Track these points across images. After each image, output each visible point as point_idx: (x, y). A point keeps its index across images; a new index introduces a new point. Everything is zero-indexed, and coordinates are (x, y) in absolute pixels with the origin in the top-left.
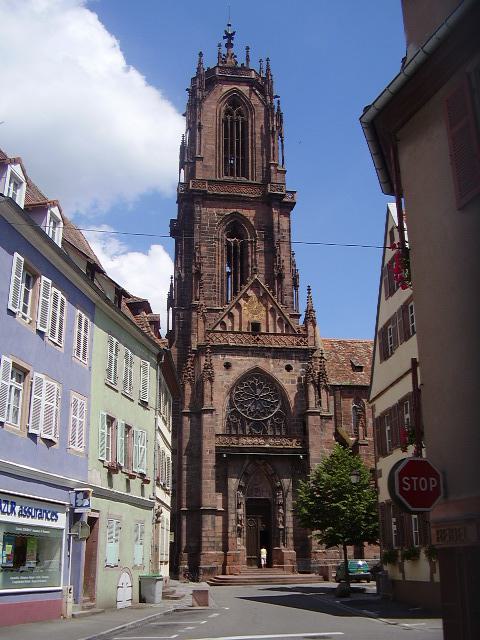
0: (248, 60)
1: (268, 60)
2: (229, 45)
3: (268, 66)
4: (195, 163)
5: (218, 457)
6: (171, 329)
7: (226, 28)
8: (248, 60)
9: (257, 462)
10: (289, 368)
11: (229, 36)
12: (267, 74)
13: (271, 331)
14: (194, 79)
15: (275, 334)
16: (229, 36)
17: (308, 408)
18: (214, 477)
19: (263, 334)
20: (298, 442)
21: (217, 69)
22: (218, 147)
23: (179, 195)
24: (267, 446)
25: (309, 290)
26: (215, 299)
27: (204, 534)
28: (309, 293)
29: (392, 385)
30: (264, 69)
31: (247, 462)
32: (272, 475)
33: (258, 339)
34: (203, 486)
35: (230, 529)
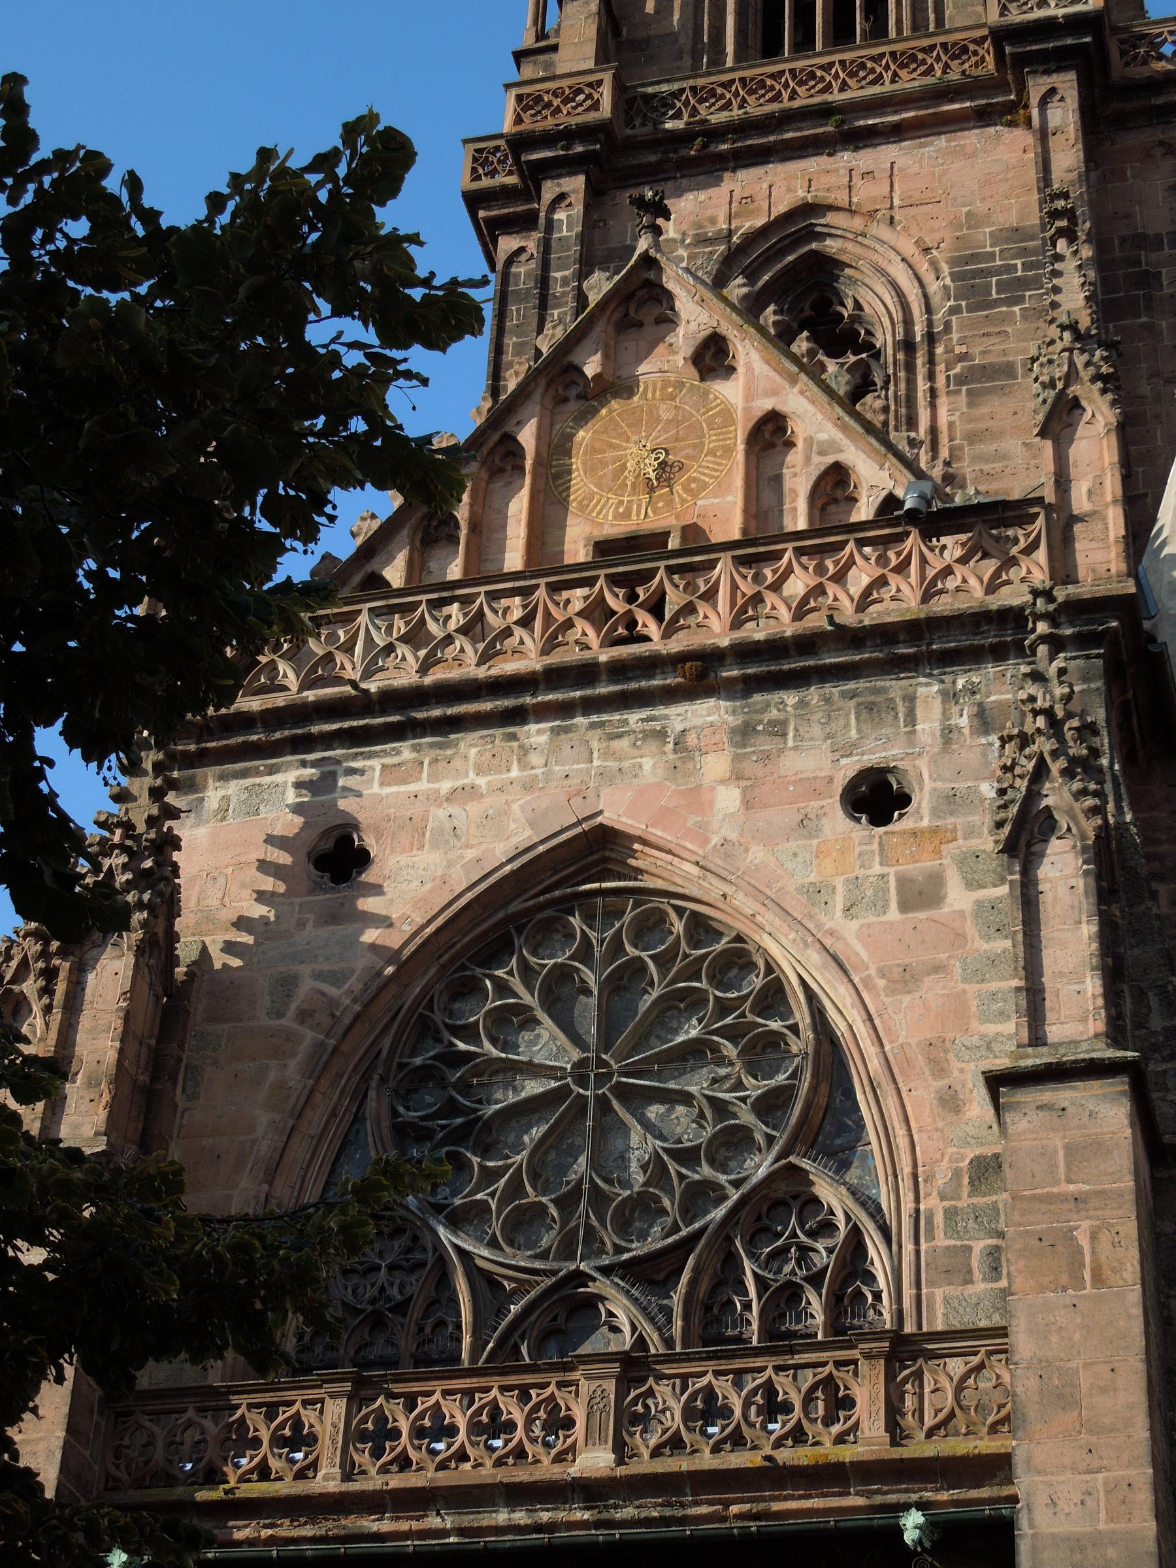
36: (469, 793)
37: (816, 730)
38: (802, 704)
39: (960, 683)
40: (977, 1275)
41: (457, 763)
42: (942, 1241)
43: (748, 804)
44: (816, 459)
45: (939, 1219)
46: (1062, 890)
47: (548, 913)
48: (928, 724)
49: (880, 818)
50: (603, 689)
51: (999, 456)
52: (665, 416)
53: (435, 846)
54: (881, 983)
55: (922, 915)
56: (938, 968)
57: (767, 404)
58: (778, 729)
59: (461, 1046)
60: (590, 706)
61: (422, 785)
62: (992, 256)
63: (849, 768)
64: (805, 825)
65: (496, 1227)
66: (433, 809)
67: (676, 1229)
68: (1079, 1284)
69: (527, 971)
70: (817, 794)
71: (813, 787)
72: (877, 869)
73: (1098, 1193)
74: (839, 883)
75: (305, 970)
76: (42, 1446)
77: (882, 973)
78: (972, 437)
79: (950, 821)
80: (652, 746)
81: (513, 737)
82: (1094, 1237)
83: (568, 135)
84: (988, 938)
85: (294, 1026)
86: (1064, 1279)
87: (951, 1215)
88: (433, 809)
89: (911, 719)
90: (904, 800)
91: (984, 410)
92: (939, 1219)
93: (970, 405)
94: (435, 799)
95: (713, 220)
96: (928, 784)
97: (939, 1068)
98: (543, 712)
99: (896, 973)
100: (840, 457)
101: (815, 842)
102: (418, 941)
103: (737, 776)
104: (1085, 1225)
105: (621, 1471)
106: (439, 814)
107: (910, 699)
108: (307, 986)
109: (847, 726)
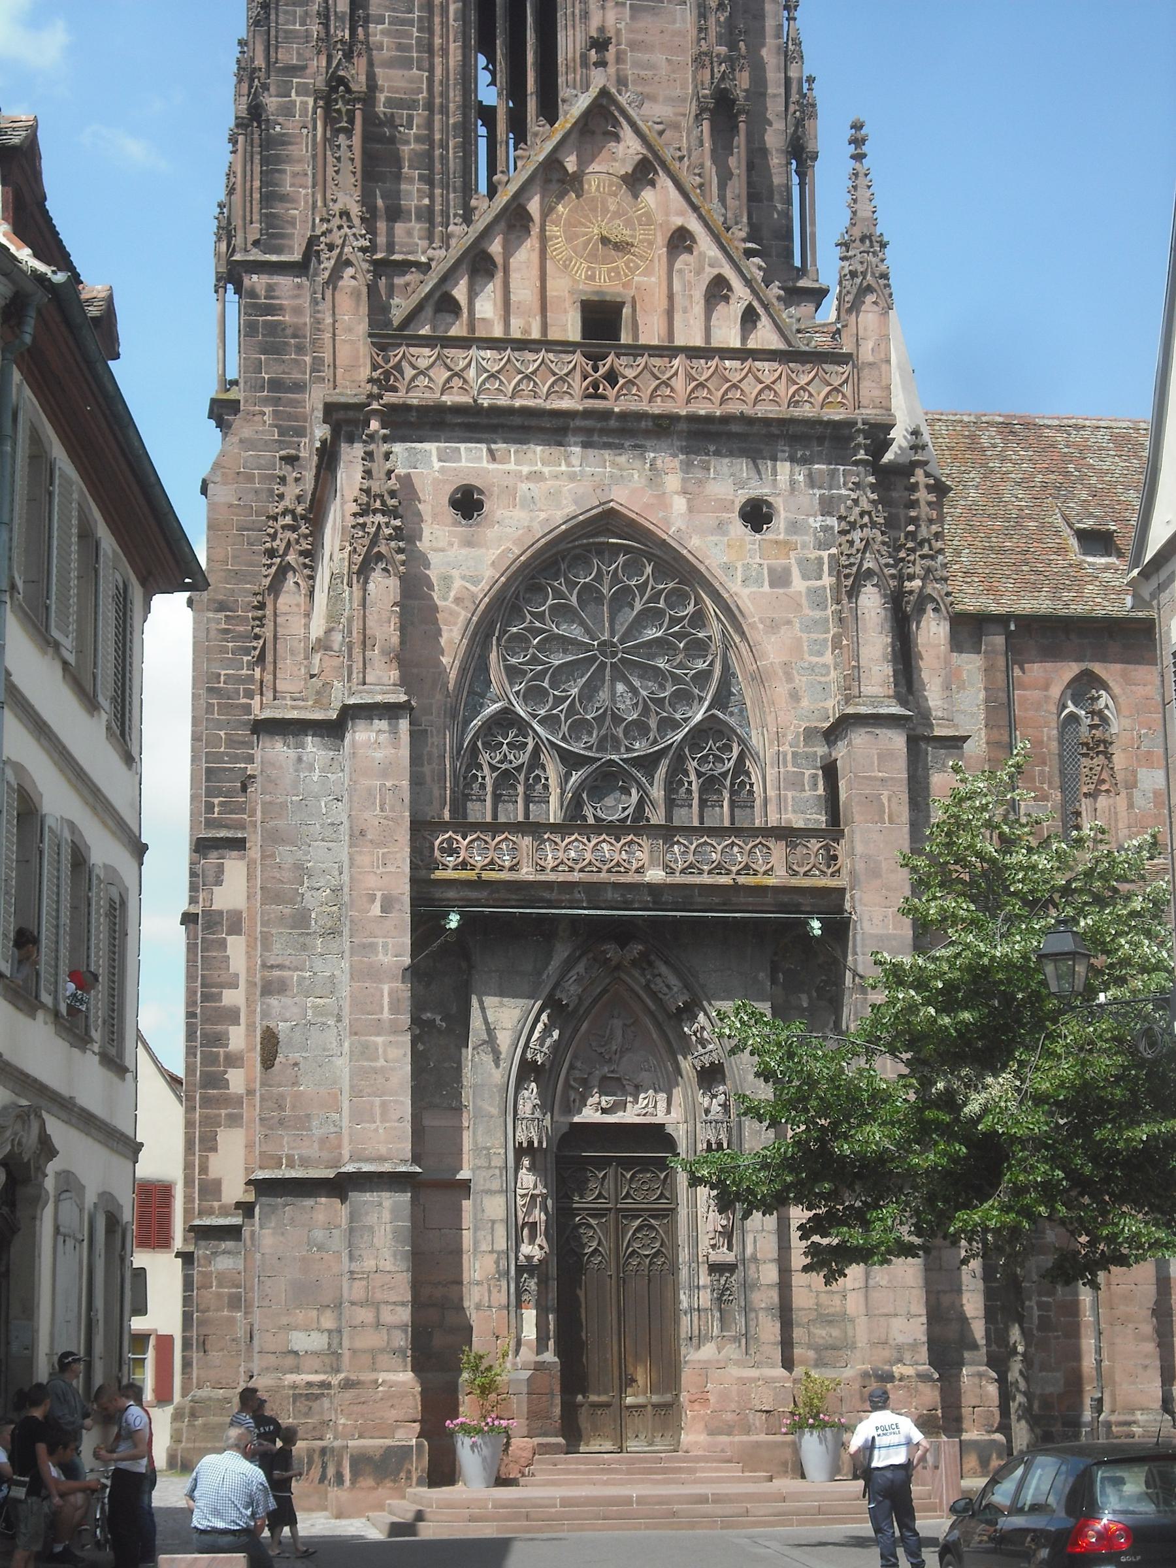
9: (611, 951)
18: (405, 1019)
24: (655, 875)
25: (858, 142)
28: (859, 157)
31: (562, 952)
33: (612, 377)
36: (536, 476)
37: (725, 470)
39: (799, 454)
40: (807, 788)
41: (530, 455)
42: (791, 768)
43: (690, 509)
44: (708, 269)
45: (789, 757)
46: (873, 614)
47: (578, 551)
49: (757, 529)
50: (613, 423)
51: (650, 66)
52: (612, 208)
53: (523, 507)
54: (761, 626)
55: (781, 591)
56: (789, 622)
57: (678, 221)
59: (538, 624)
60: (603, 432)
61: (511, 466)
63: (742, 496)
64: (721, 527)
65: (565, 729)
66: (519, 484)
67: (655, 742)
69: (572, 585)
70: (727, 510)
71: (725, 507)
72: (758, 560)
73: (892, 778)
74: (739, 565)
75: (455, 573)
76: (398, 855)
77: (761, 621)
78: (633, 45)
79: (794, 538)
82: (889, 800)
84: (813, 609)
85: (453, 606)
86: (877, 818)
87: (794, 754)
88: (519, 484)
90: (768, 519)
91: (641, 24)
93: (632, 17)
94: (518, 474)
97: (789, 678)
98: (578, 430)
99: (768, 622)
100: (722, 271)
101: (726, 539)
102: (517, 563)
104: (886, 793)
105: (669, 880)
106: (523, 487)
108: (458, 584)
109: (741, 469)
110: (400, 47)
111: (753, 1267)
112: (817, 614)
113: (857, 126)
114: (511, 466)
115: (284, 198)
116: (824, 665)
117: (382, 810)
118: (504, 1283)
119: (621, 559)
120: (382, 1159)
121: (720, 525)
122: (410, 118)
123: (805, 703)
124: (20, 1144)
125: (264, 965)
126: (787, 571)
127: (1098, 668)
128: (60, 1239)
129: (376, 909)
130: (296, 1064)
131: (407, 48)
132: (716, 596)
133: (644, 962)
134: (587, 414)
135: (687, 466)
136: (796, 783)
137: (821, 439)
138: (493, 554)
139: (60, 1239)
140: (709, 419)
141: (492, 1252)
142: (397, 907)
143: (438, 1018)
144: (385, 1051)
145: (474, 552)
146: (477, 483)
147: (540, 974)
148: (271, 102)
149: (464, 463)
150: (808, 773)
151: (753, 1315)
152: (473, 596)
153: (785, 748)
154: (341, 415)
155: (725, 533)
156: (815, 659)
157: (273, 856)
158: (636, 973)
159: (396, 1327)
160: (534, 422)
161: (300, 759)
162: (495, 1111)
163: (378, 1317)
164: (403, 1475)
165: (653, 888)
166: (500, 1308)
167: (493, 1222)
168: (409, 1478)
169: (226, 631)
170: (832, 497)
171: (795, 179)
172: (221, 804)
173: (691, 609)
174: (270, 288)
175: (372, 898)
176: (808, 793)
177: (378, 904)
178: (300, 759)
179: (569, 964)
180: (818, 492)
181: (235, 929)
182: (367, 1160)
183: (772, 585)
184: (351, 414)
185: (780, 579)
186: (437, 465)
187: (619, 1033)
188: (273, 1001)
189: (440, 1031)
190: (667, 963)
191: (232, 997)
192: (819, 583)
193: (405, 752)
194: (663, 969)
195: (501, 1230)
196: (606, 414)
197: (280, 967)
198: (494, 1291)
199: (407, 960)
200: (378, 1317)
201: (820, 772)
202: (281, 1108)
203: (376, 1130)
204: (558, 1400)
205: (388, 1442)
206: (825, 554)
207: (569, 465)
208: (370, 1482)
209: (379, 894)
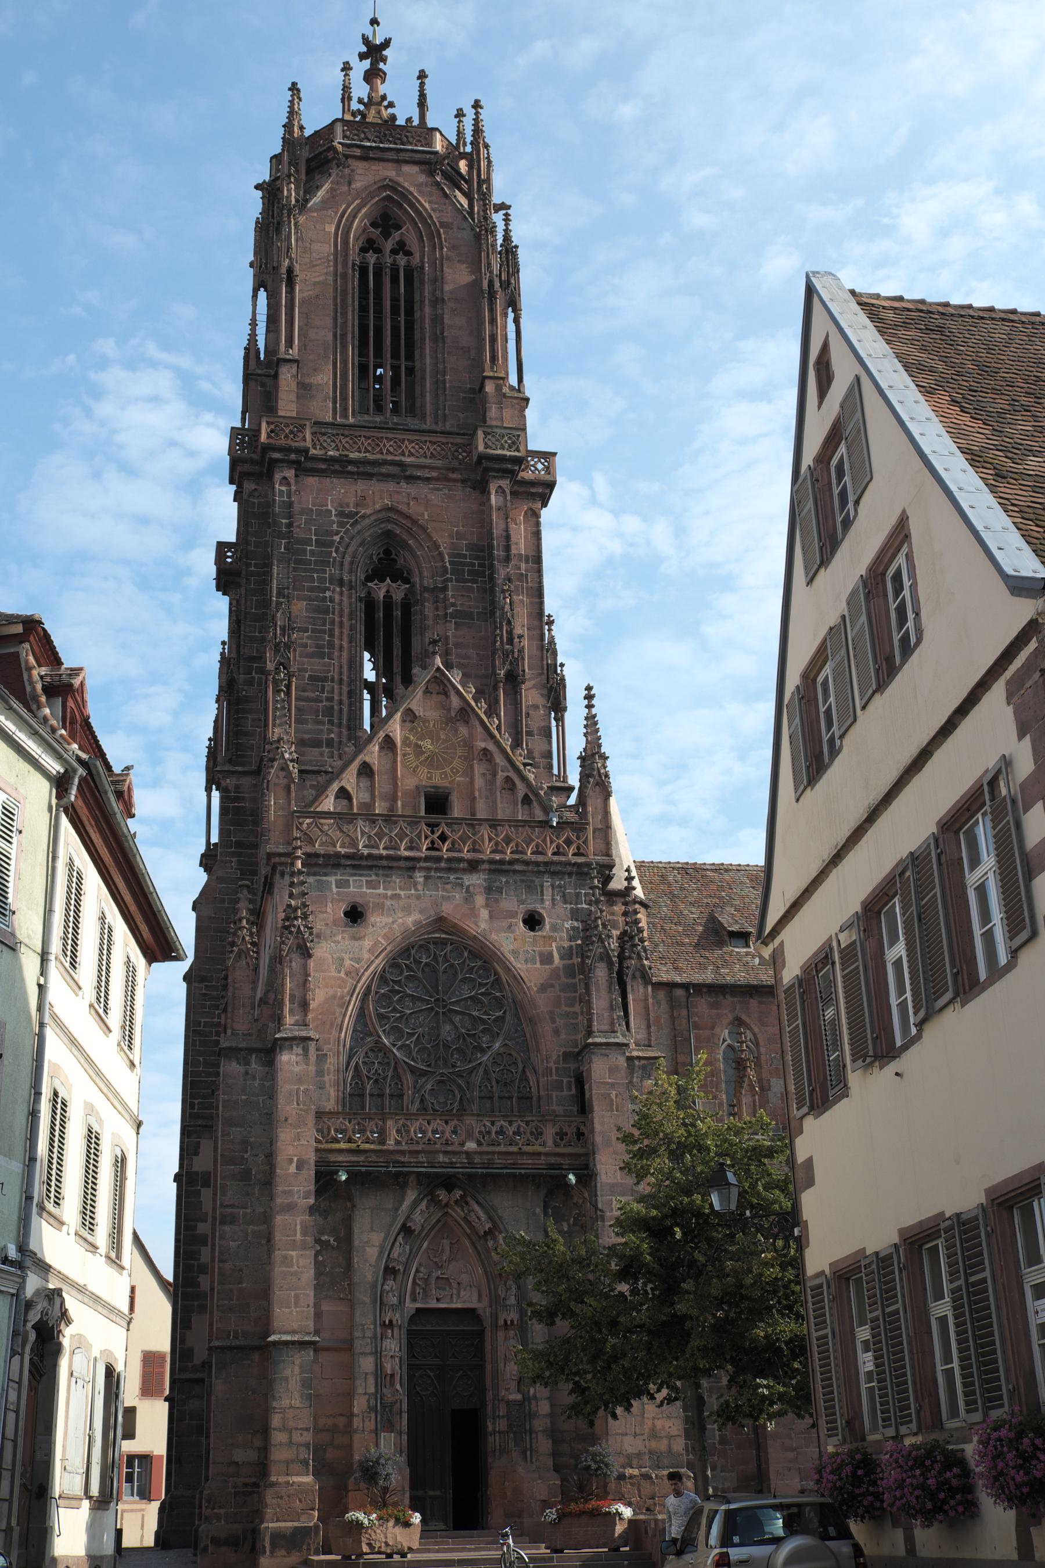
0: (422, 103)
1: (477, 105)
2: (373, 75)
3: (477, 121)
4: (276, 376)
5: (324, 1178)
6: (215, 839)
7: (368, 31)
8: (422, 103)
9: (442, 1194)
10: (533, 921)
11: (374, 52)
12: (475, 144)
13: (481, 814)
14: (276, 159)
15: (494, 824)
16: (374, 52)
17: (590, 1033)
18: (310, 1240)
19: (458, 821)
20: (561, 1135)
21: (339, 129)
22: (339, 338)
23: (235, 462)
25: (589, 697)
26: (330, 743)
27: (276, 1421)
28: (590, 707)
29: (837, 859)
30: (469, 138)
31: (411, 1196)
32: (490, 1233)
34: (278, 1270)
35: (359, 1404)
37: (512, 893)
38: (507, 882)
41: (392, 884)
42: (555, 1077)
43: (491, 917)
44: (500, 773)
45: (554, 1070)
48: (547, 897)
49: (532, 928)
50: (443, 865)
58: (500, 891)
59: (397, 988)
60: (437, 869)
61: (381, 891)
62: (465, 556)
68: (612, 1111)
75: (346, 957)
80: (458, 889)
81: (411, 877)
83: (289, 450)
87: (557, 1069)
89: (542, 894)
92: (554, 1070)
93: (456, 629)
94: (385, 896)
95: (348, 505)
96: (547, 920)
97: (553, 1021)
98: (421, 869)
103: (487, 906)
106: (388, 903)
107: (542, 886)
108: (347, 963)
110: (318, 646)
111: (533, 1402)
112: (570, 981)
113: (589, 688)
114: (381, 891)
115: (247, 734)
116: (575, 1013)
117: (298, 1104)
118: (373, 1416)
119: (449, 948)
120: (294, 1332)
121: (510, 926)
122: (323, 687)
123: (563, 1036)
124: (47, 1314)
125: (221, 1205)
126: (551, 954)
127: (744, 1017)
128: (73, 1380)
129: (293, 1168)
130: (241, 1270)
131: (323, 646)
132: (508, 969)
133: (462, 1202)
134: (427, 859)
135: (489, 890)
136: (558, 1086)
137: (570, 874)
138: (368, 943)
139: (73, 1380)
140: (502, 862)
141: (365, 1394)
142: (306, 1167)
143: (332, 1240)
144: (298, 1261)
145: (357, 943)
146: (359, 900)
147: (397, 1210)
148: (242, 678)
149: (351, 889)
150: (565, 1080)
151: (534, 1435)
152: (357, 971)
153: (552, 1065)
154: (277, 860)
155: (513, 932)
156: (568, 1009)
157: (228, 1134)
158: (458, 1210)
159: (302, 1445)
160: (395, 864)
161: (247, 1073)
162: (367, 1300)
163: (290, 1437)
164: (305, 1547)
165: (468, 1154)
166: (371, 1432)
167: (366, 1374)
168: (309, 1549)
169: (205, 995)
170: (577, 909)
171: (554, 723)
172: (199, 1103)
173: (492, 978)
174: (237, 787)
175: (291, 1161)
176: (565, 1093)
177: (294, 1165)
178: (247, 1073)
179: (415, 1204)
180: (569, 906)
181: (206, 1184)
182: (286, 1333)
183: (542, 963)
184: (283, 859)
185: (547, 959)
186: (335, 890)
187: (447, 1249)
188: (227, 1228)
189: (333, 1248)
190: (478, 1202)
191: (203, 1228)
192: (570, 962)
193: (312, 1068)
194: (476, 1207)
195: (371, 1380)
196: (439, 859)
197: (232, 1206)
198: (367, 1420)
199: (312, 1201)
200: (290, 1437)
201: (573, 1080)
202: (231, 1299)
203: (291, 1313)
204: (407, 1495)
205: (296, 1524)
206: (573, 943)
207: (416, 890)
208: (283, 1552)
209: (295, 1159)
